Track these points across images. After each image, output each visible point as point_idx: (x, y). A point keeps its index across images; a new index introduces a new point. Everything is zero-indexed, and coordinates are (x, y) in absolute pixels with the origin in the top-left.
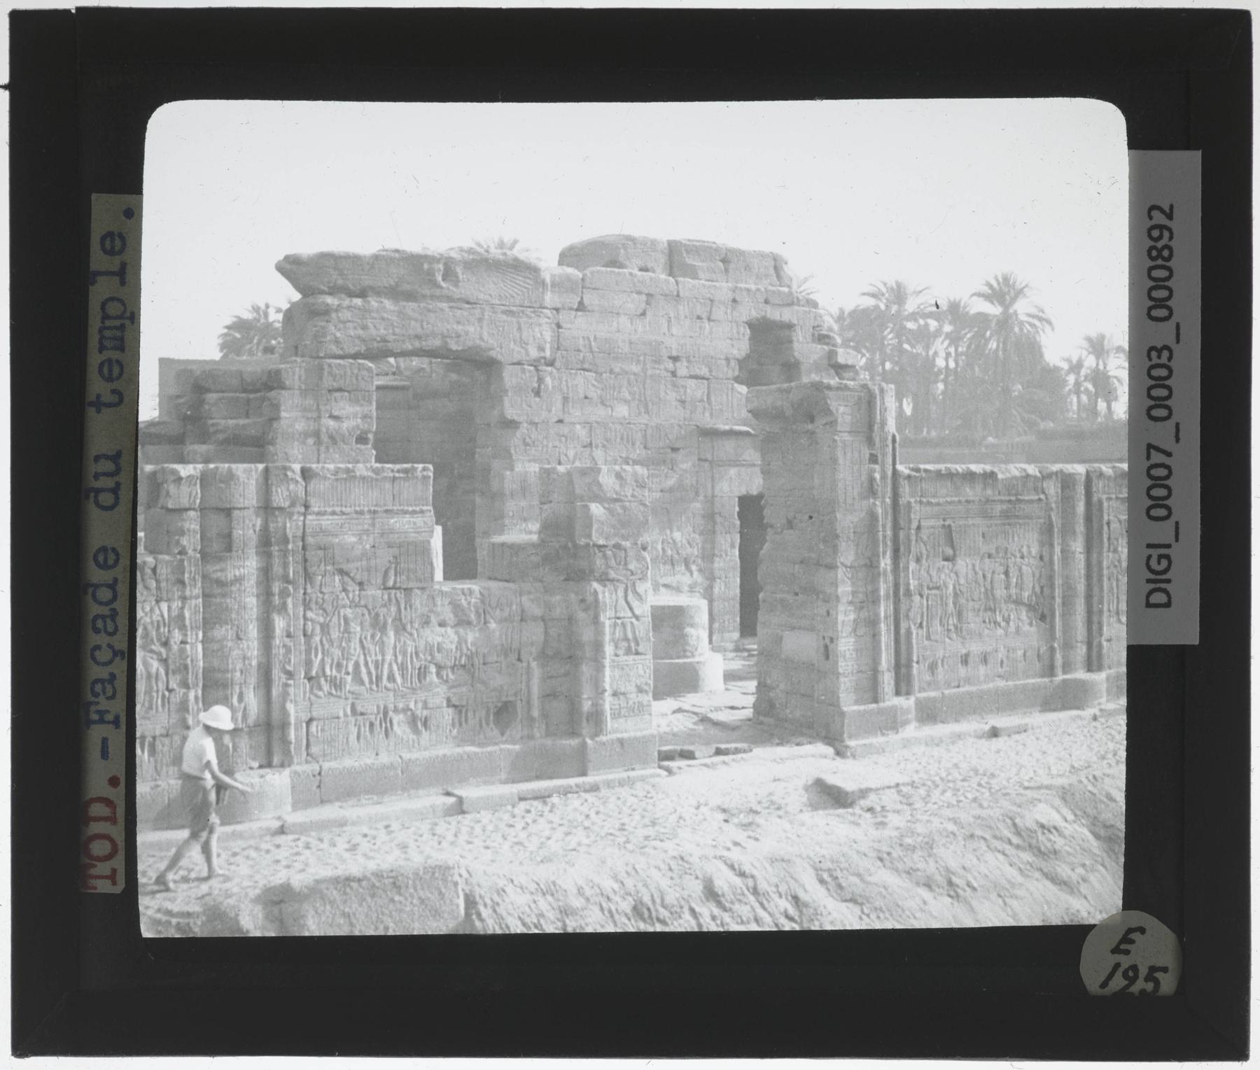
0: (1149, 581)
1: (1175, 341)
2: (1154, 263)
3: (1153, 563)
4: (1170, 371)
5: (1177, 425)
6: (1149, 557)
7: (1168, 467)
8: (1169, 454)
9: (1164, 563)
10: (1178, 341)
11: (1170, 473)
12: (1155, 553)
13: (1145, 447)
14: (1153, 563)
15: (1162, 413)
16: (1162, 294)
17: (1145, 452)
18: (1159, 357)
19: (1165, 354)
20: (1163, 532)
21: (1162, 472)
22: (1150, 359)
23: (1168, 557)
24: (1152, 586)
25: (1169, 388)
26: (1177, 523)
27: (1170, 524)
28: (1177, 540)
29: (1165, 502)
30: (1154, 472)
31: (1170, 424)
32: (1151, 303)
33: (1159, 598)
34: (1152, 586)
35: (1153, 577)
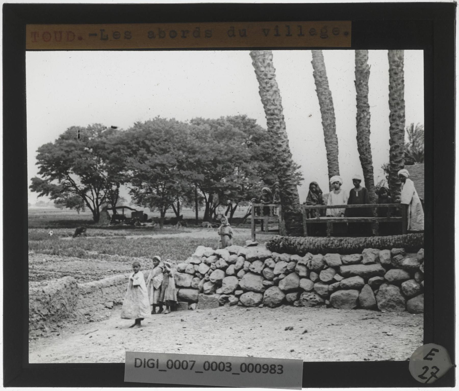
0: (145, 359)
2: (262, 366)
3: (151, 361)
5: (202, 372)
6: (154, 360)
8: (191, 369)
10: (233, 374)
13: (194, 360)
18: (227, 367)
19: (228, 369)
22: (227, 363)
23: (153, 367)
25: (216, 370)
28: (160, 370)
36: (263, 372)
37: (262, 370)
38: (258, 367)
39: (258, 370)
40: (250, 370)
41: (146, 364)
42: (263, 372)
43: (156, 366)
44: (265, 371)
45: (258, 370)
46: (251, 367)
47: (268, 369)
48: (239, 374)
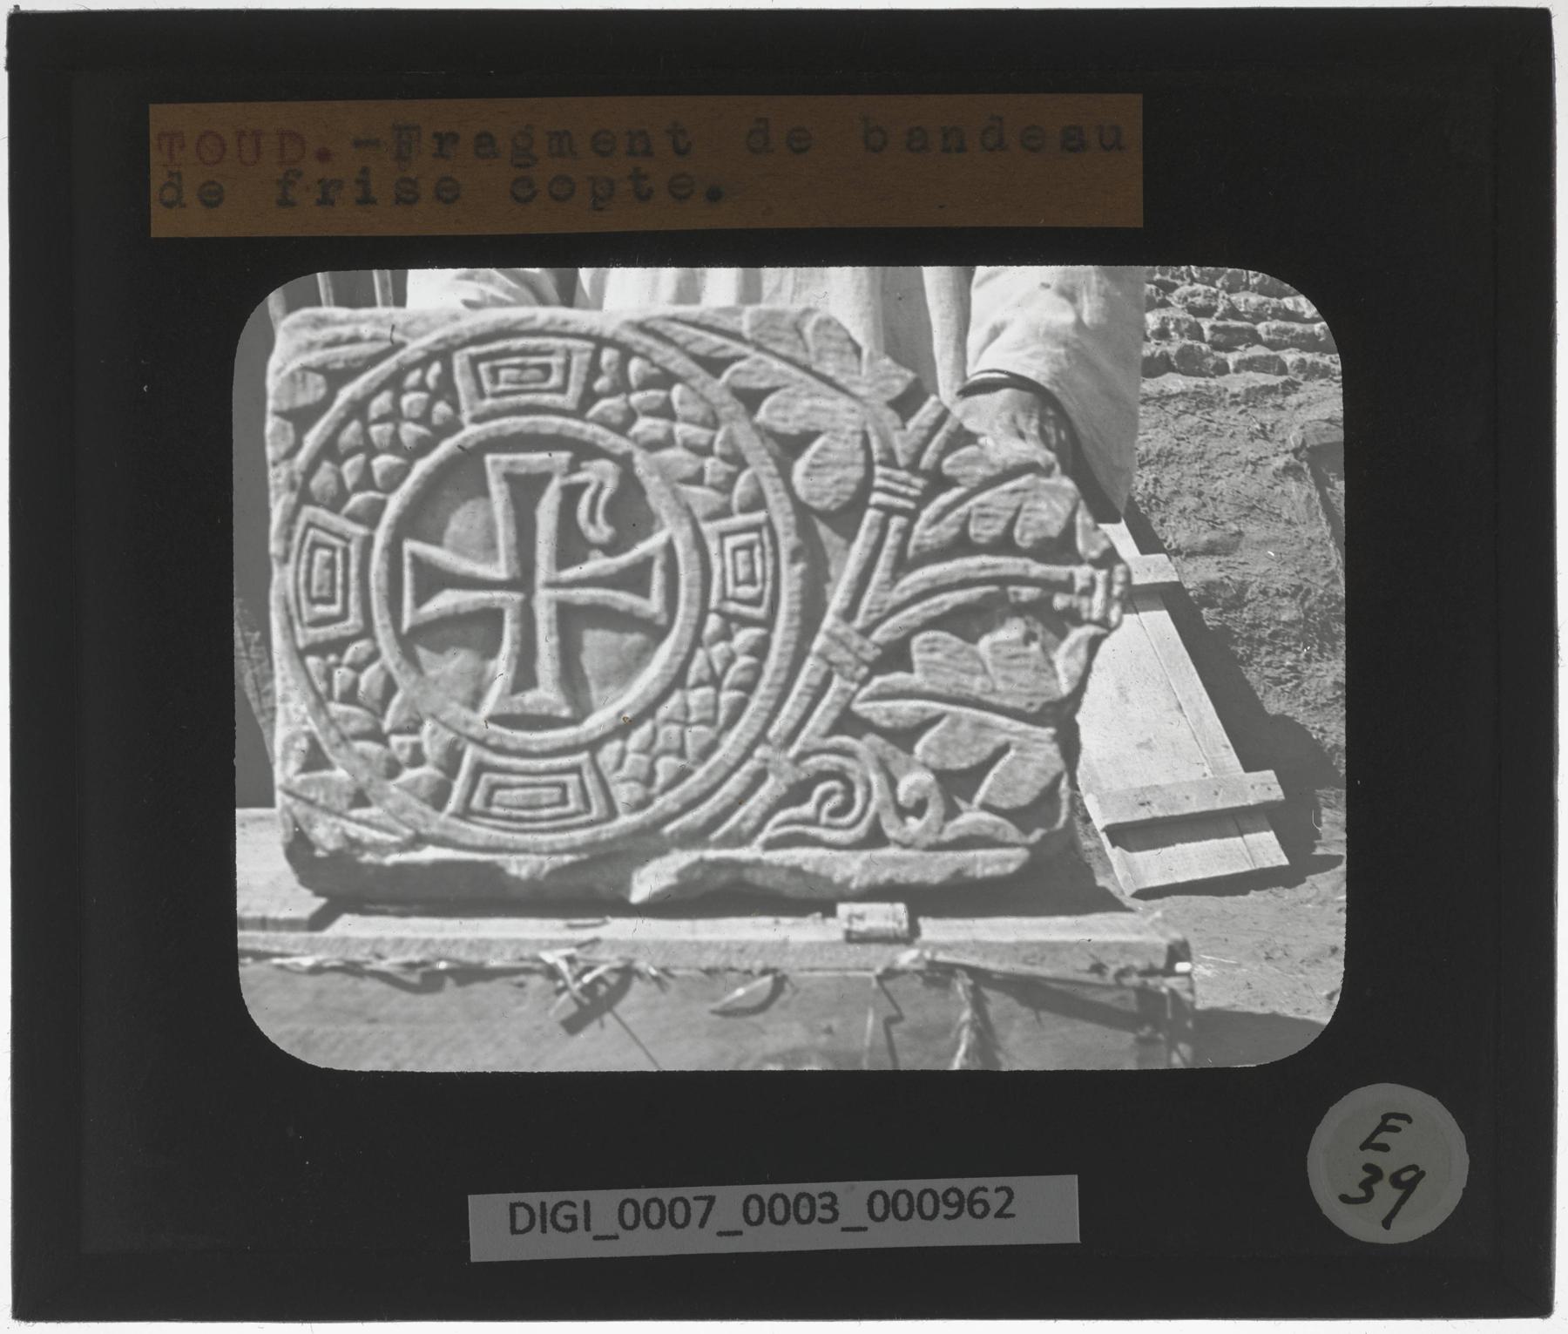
0: (543, 1205)
1: (845, 1226)
2: (941, 1199)
3: (566, 1210)
4: (809, 1221)
6: (573, 1205)
7: (682, 1226)
8: (702, 1224)
9: (567, 1224)
10: (844, 1229)
11: (677, 1226)
12: (579, 1212)
14: (566, 1210)
15: (754, 1214)
16: (903, 1209)
18: (824, 1207)
19: (828, 1214)
21: (680, 1219)
22: (821, 1196)
23: (574, 1228)
26: (616, 1237)
28: (596, 1238)
30: (679, 1207)
31: (740, 1224)
33: (523, 1219)
35: (549, 1212)
36: (947, 1217)
37: (944, 1209)
38: (928, 1200)
39: (928, 1210)
40: (903, 1210)
41: (548, 1218)
42: (947, 1217)
43: (581, 1223)
44: (953, 1211)
45: (928, 1210)
46: (903, 1201)
47: (960, 1205)
48: (865, 1229)
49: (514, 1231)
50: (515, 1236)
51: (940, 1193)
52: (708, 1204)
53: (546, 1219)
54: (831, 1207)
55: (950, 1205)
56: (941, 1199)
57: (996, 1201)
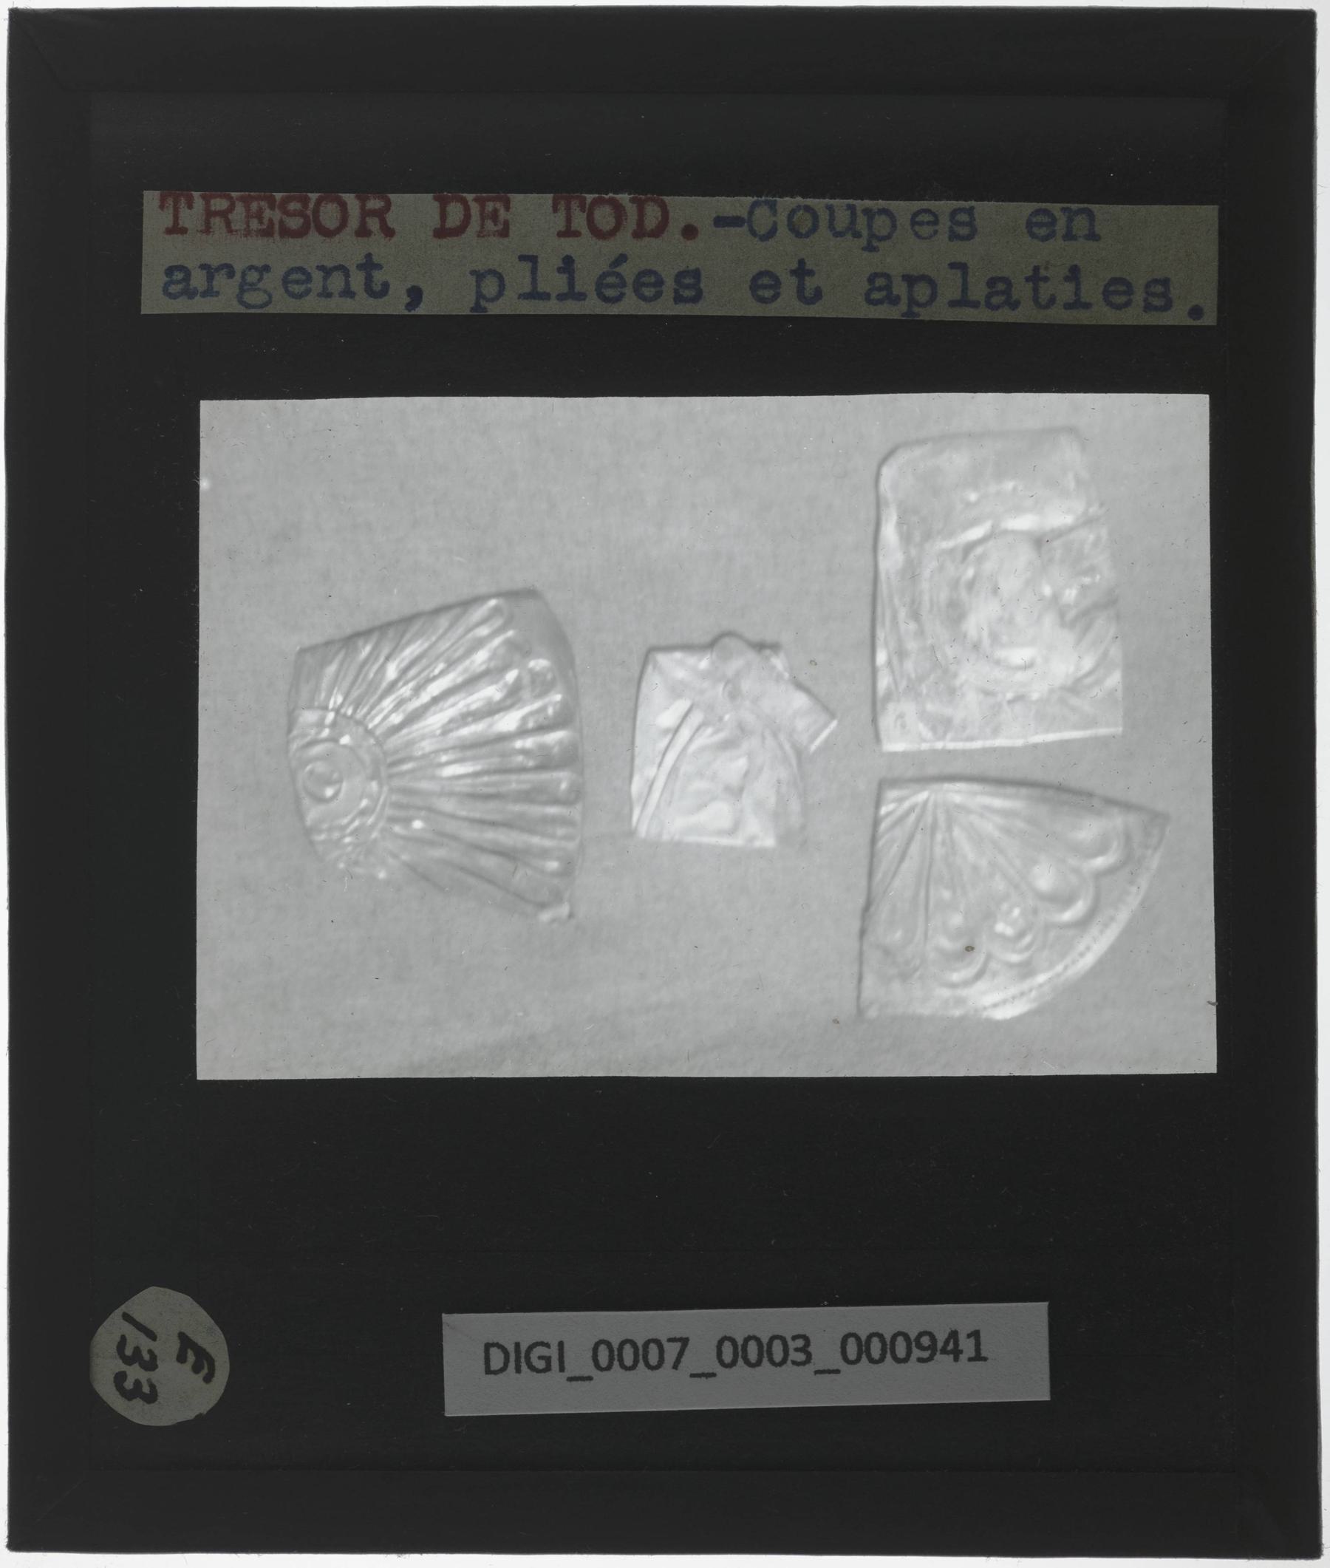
0: (517, 1345)
4: (780, 1364)
5: (713, 1375)
6: (547, 1345)
8: (675, 1366)
9: (541, 1365)
10: (817, 1372)
13: (684, 1336)
15: (728, 1357)
17: (678, 1336)
18: (797, 1350)
19: (801, 1357)
20: (579, 1361)
21: (653, 1359)
22: (794, 1338)
23: (548, 1368)
24: (511, 1349)
26: (590, 1378)
27: (589, 1369)
28: (571, 1379)
29: (641, 1361)
30: (653, 1350)
32: (863, 1338)
33: (497, 1359)
34: (511, 1349)
35: (523, 1355)
37: (917, 1353)
41: (523, 1360)
42: (920, 1360)
44: (926, 1354)
45: (901, 1351)
47: (933, 1348)
48: (837, 1372)
49: (488, 1371)
50: (489, 1376)
51: (913, 1336)
52: (682, 1346)
53: (520, 1358)
54: (804, 1350)
55: (923, 1349)
56: (914, 1344)
57: (967, 1346)
